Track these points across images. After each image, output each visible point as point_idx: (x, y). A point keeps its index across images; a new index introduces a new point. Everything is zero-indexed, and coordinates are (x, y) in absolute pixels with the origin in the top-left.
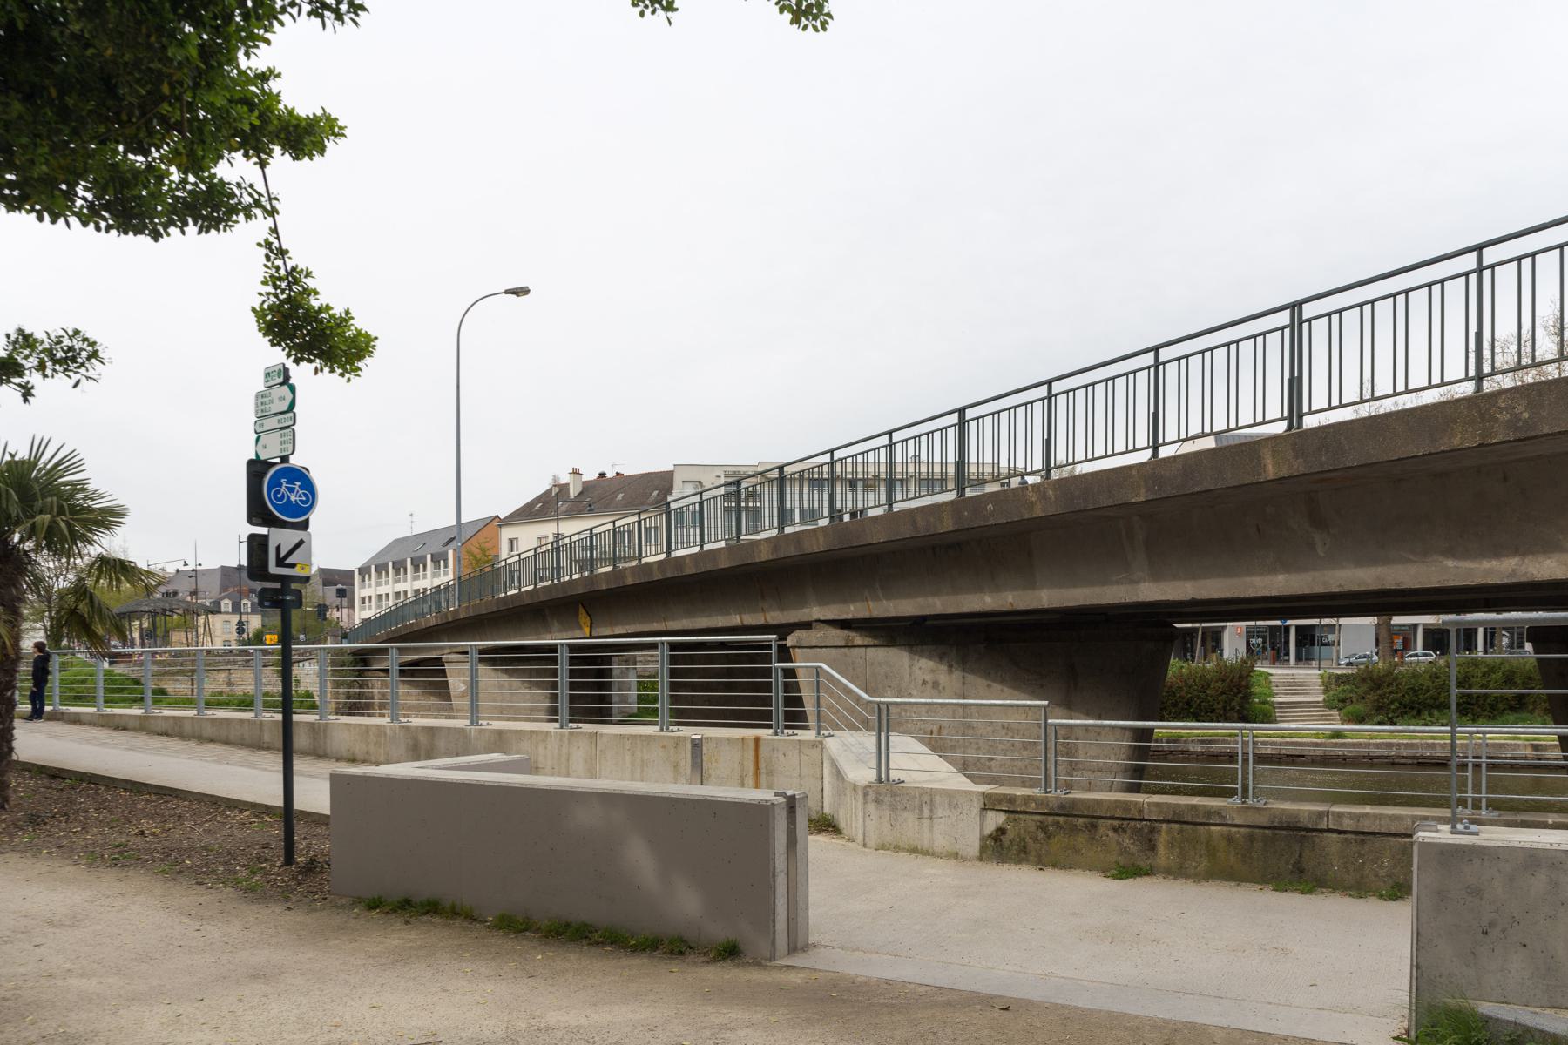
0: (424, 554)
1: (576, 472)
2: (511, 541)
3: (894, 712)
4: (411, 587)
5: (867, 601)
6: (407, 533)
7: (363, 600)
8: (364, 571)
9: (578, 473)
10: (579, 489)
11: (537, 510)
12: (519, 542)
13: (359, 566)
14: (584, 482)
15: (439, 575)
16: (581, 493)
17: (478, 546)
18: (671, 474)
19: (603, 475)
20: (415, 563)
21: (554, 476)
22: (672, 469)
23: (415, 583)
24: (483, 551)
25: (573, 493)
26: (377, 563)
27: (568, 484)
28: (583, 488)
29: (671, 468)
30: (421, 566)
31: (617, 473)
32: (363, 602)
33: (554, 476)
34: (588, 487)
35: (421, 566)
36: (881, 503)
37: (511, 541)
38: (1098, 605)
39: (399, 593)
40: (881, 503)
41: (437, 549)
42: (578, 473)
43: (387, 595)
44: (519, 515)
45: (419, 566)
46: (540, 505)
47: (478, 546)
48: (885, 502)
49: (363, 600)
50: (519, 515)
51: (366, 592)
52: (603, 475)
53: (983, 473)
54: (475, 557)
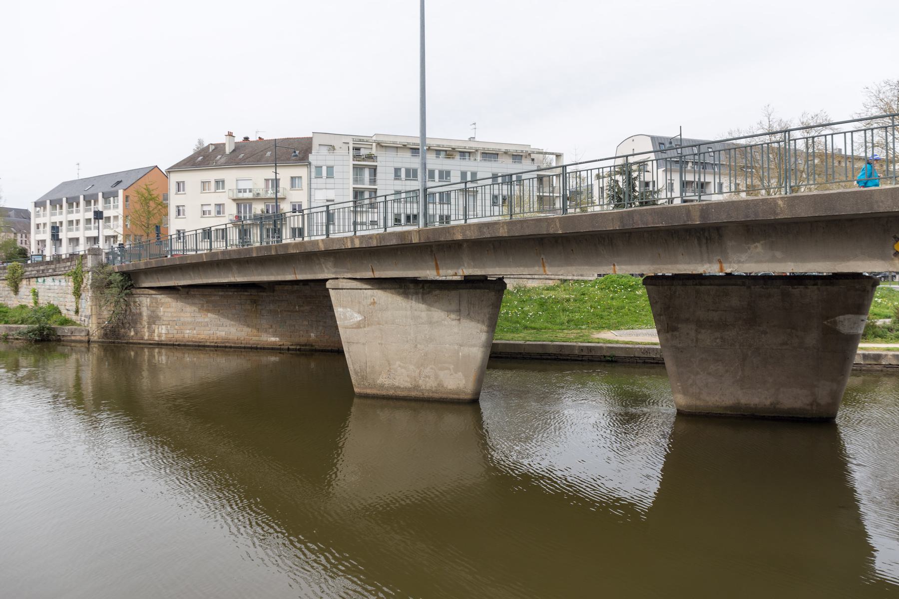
0: (95, 192)
1: (230, 135)
2: (178, 183)
3: (668, 336)
4: (84, 217)
5: (544, 267)
6: (73, 177)
7: (38, 226)
8: (39, 204)
9: (232, 136)
10: (233, 148)
11: (199, 161)
12: (186, 186)
13: (34, 201)
14: (236, 143)
15: (110, 208)
16: (234, 151)
17: (145, 187)
18: (311, 139)
19: (246, 139)
20: (87, 199)
21: (199, 140)
22: (311, 136)
23: (69, 215)
24: (148, 190)
25: (228, 150)
26: (52, 198)
27: (224, 144)
28: (235, 147)
29: (311, 135)
30: (75, 204)
31: (260, 138)
32: (38, 228)
33: (199, 140)
34: (238, 148)
35: (75, 204)
36: (381, 227)
37: (178, 183)
38: (849, 273)
39: (72, 221)
40: (381, 227)
41: (108, 189)
42: (232, 136)
43: (45, 224)
44: (185, 164)
45: (90, 202)
46: (201, 158)
47: (145, 187)
48: (383, 227)
49: (38, 226)
50: (185, 164)
51: (40, 220)
52: (246, 139)
53: (580, 187)
54: (143, 196)
